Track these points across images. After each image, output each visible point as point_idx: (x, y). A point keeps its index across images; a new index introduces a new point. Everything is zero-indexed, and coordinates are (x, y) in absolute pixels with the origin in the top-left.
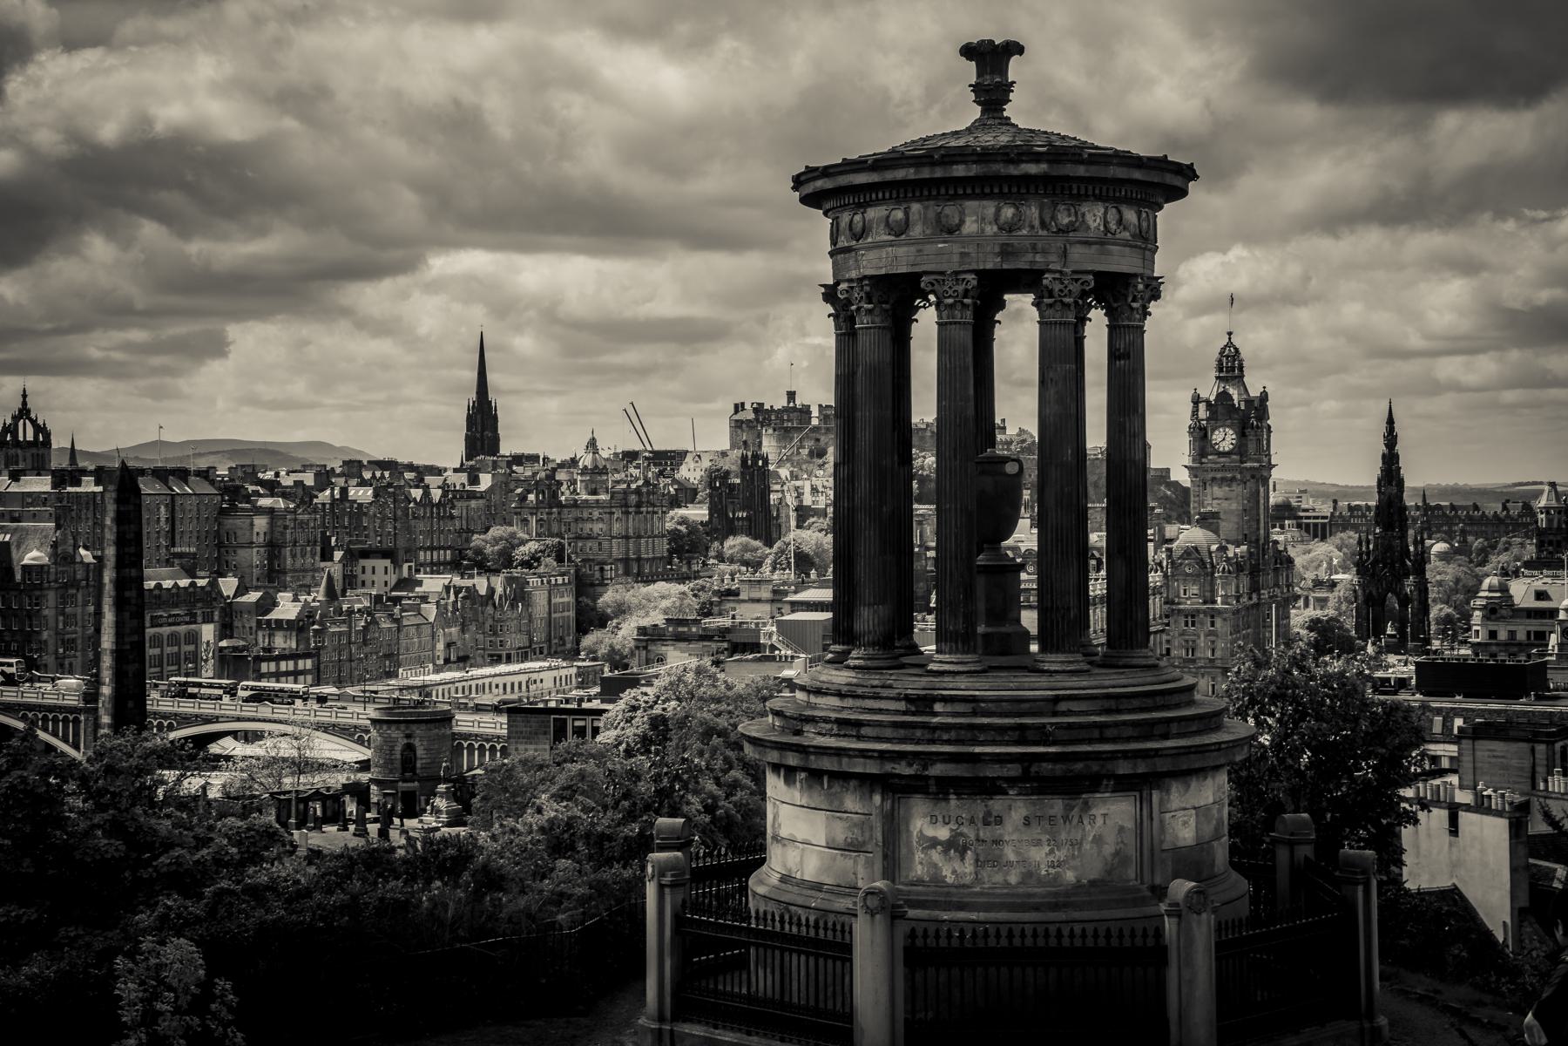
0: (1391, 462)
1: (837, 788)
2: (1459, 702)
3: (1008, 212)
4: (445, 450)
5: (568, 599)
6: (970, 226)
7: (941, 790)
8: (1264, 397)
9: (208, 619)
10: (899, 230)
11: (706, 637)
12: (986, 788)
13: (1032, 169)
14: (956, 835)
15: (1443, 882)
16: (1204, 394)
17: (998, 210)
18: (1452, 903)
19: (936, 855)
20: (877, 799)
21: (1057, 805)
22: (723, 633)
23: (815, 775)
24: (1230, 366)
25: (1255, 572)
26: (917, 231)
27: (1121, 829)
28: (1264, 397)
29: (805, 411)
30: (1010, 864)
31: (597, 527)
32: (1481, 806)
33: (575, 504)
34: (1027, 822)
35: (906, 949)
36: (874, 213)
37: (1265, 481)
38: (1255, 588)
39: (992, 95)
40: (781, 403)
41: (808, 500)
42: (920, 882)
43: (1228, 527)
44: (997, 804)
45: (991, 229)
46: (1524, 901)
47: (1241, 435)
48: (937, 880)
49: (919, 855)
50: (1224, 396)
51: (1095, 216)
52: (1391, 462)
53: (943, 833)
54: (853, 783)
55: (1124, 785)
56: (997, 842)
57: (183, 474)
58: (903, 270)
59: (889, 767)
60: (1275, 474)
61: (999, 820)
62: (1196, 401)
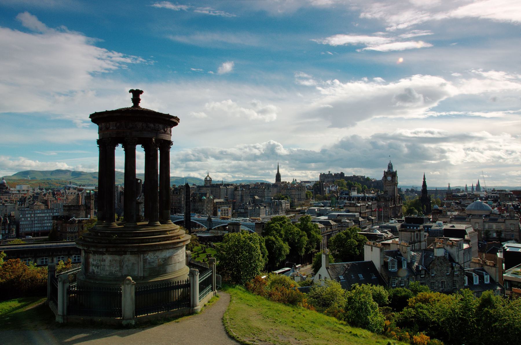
0: (424, 183)
2: (412, 224)
3: (118, 124)
4: (273, 181)
5: (289, 204)
6: (111, 128)
7: (95, 253)
8: (396, 171)
9: (230, 207)
11: (297, 211)
12: (102, 253)
13: (118, 114)
15: (370, 260)
16: (386, 170)
17: (116, 124)
18: (371, 264)
19: (94, 268)
21: (117, 258)
22: (299, 211)
24: (390, 167)
25: (394, 201)
27: (133, 264)
28: (396, 171)
29: (331, 174)
30: (107, 270)
31: (294, 193)
32: (376, 246)
33: (290, 189)
34: (110, 261)
35: (68, 290)
37: (397, 186)
38: (394, 204)
40: (327, 173)
41: (331, 189)
43: (390, 193)
44: (104, 257)
45: (115, 128)
46: (383, 264)
47: (392, 178)
49: (91, 268)
50: (389, 171)
51: (140, 125)
52: (424, 183)
53: (95, 263)
55: (132, 253)
56: (104, 265)
57: (228, 185)
60: (398, 185)
61: (105, 261)
62: (385, 172)
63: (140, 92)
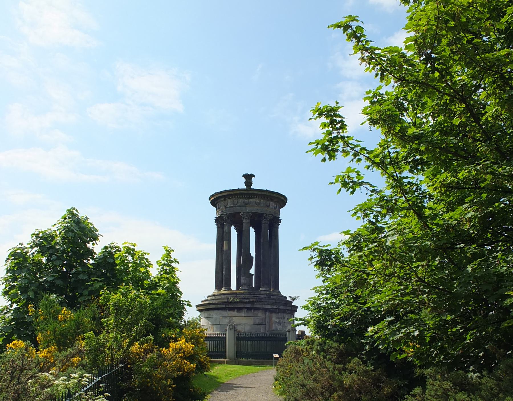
1: (256, 312)
6: (271, 207)
10: (258, 204)
14: (279, 321)
19: (277, 325)
20: (268, 313)
23: (249, 309)
26: (262, 205)
36: (251, 200)
39: (249, 183)
42: (274, 330)
48: (277, 330)
49: (274, 325)
53: (277, 320)
54: (260, 311)
58: (259, 212)
59: (273, 307)
63: (252, 176)
